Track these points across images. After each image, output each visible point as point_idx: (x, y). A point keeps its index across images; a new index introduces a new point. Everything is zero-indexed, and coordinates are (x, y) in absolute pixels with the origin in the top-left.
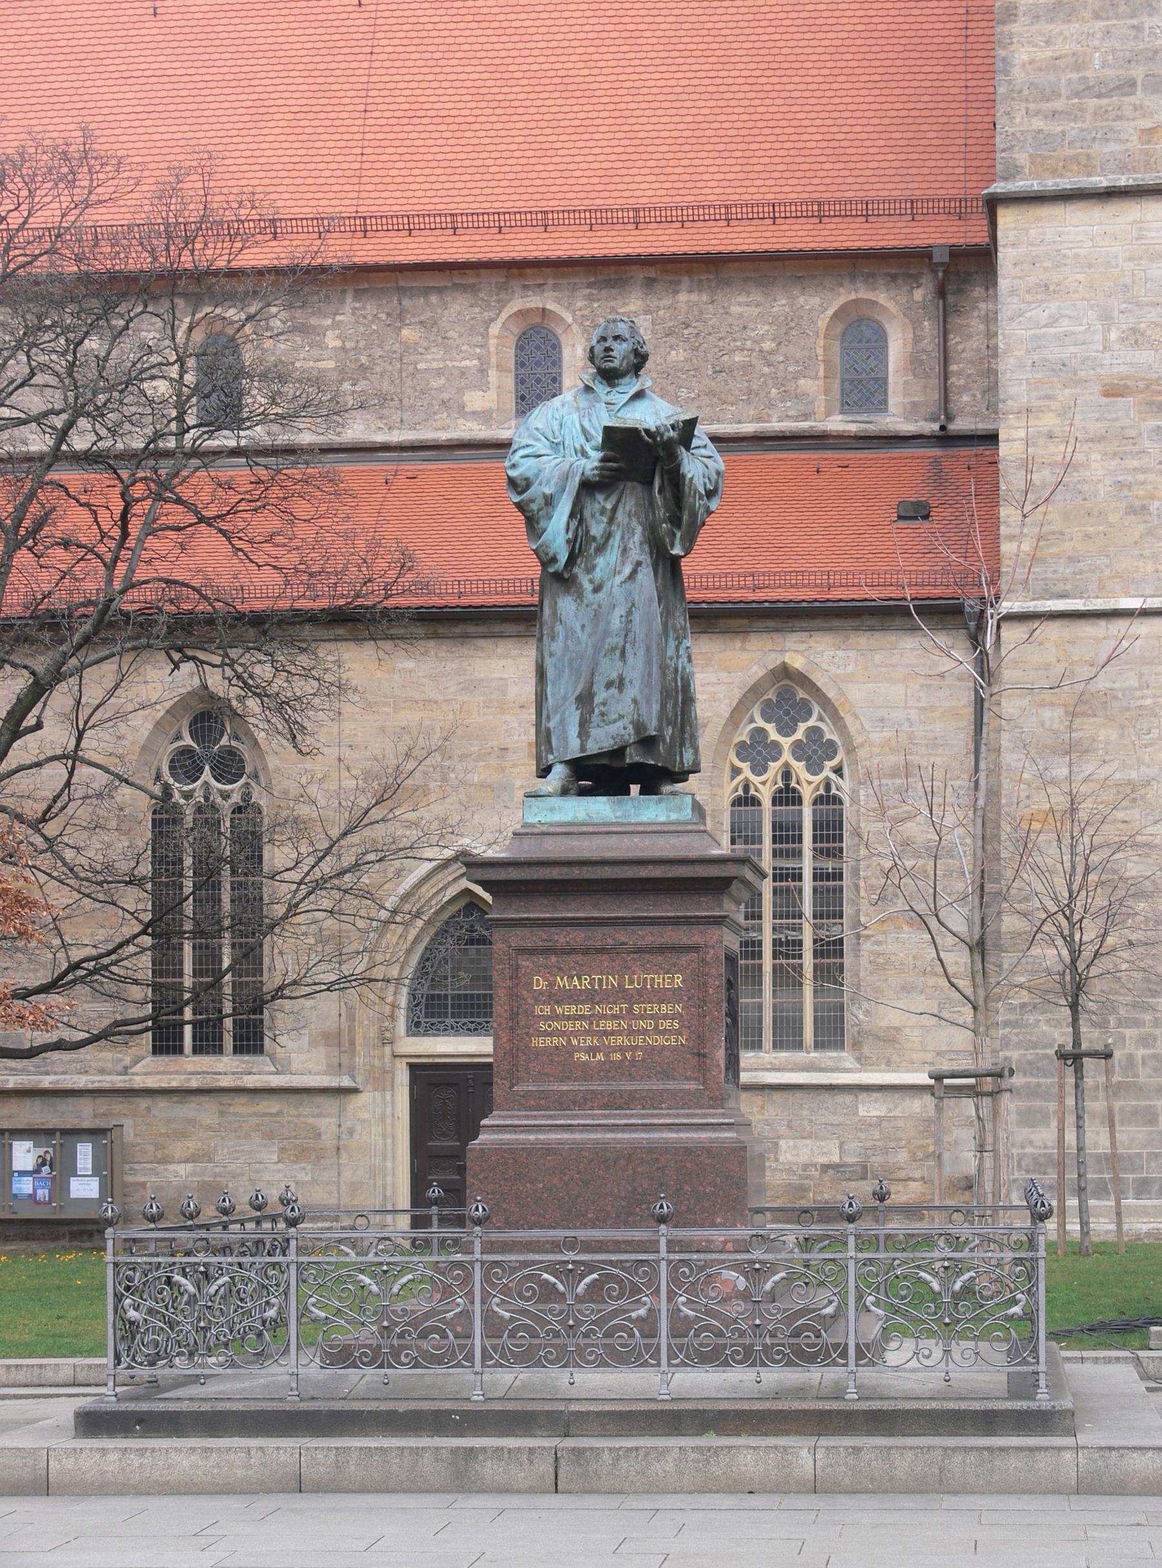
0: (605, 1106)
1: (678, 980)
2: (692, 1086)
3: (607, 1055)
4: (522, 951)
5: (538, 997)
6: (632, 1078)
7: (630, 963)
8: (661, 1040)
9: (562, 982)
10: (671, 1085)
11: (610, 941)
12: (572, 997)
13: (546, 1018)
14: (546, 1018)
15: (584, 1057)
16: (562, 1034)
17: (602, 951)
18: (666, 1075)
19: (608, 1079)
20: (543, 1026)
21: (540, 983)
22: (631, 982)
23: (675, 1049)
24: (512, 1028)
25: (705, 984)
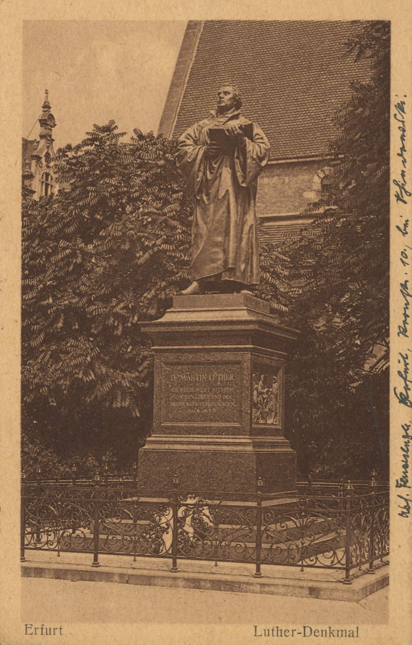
6: (211, 421)
22: (212, 378)
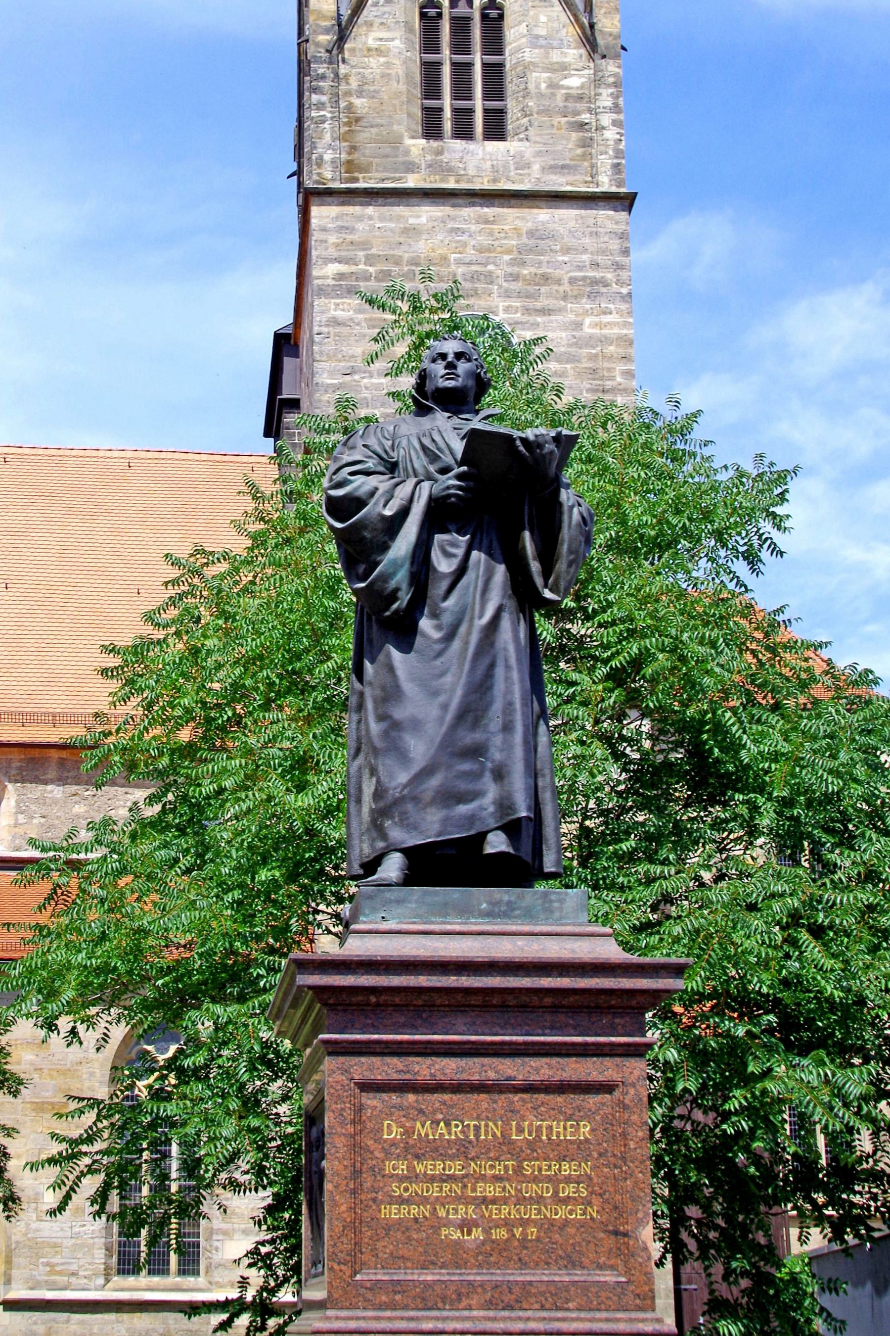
0: (490, 1305)
1: (585, 1129)
2: (609, 1277)
4: (367, 1087)
5: (389, 1149)
6: (523, 1264)
7: (518, 1105)
8: (562, 1213)
9: (423, 1129)
10: (579, 1275)
11: (492, 1075)
12: (435, 1150)
13: (401, 1179)
14: (401, 1179)
15: (456, 1235)
16: (424, 1201)
18: (572, 1263)
19: (490, 1266)
21: (392, 1132)
22: (520, 1130)
23: (581, 1225)
24: (354, 1192)
25: (624, 1135)
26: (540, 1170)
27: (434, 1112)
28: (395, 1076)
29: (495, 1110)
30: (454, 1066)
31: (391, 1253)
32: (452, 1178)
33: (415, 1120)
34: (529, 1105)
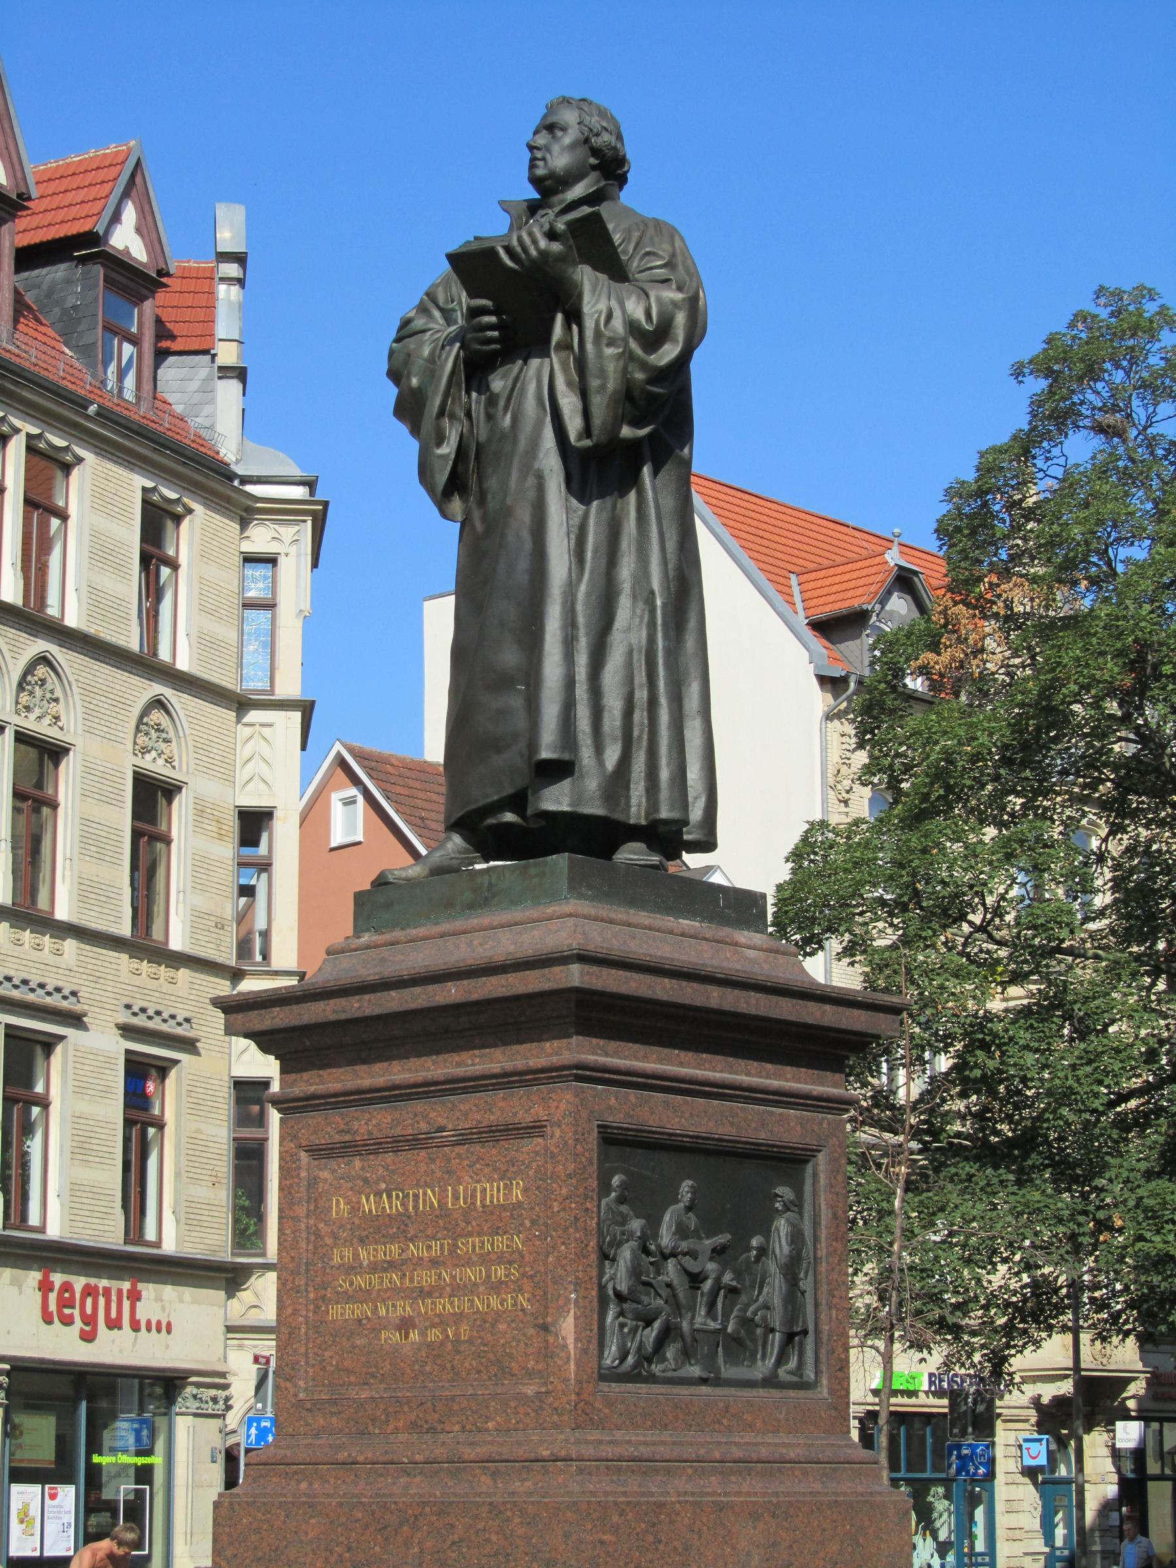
3: (423, 1334)
8: (494, 1302)
9: (368, 1205)
11: (424, 1126)
14: (352, 1269)
17: (415, 1142)
20: (343, 1284)
21: (339, 1207)
22: (456, 1198)
26: (474, 1247)
27: (377, 1182)
28: (337, 1138)
29: (433, 1172)
30: (389, 1119)
31: (337, 1365)
32: (391, 1265)
33: (360, 1193)
34: (466, 1162)
